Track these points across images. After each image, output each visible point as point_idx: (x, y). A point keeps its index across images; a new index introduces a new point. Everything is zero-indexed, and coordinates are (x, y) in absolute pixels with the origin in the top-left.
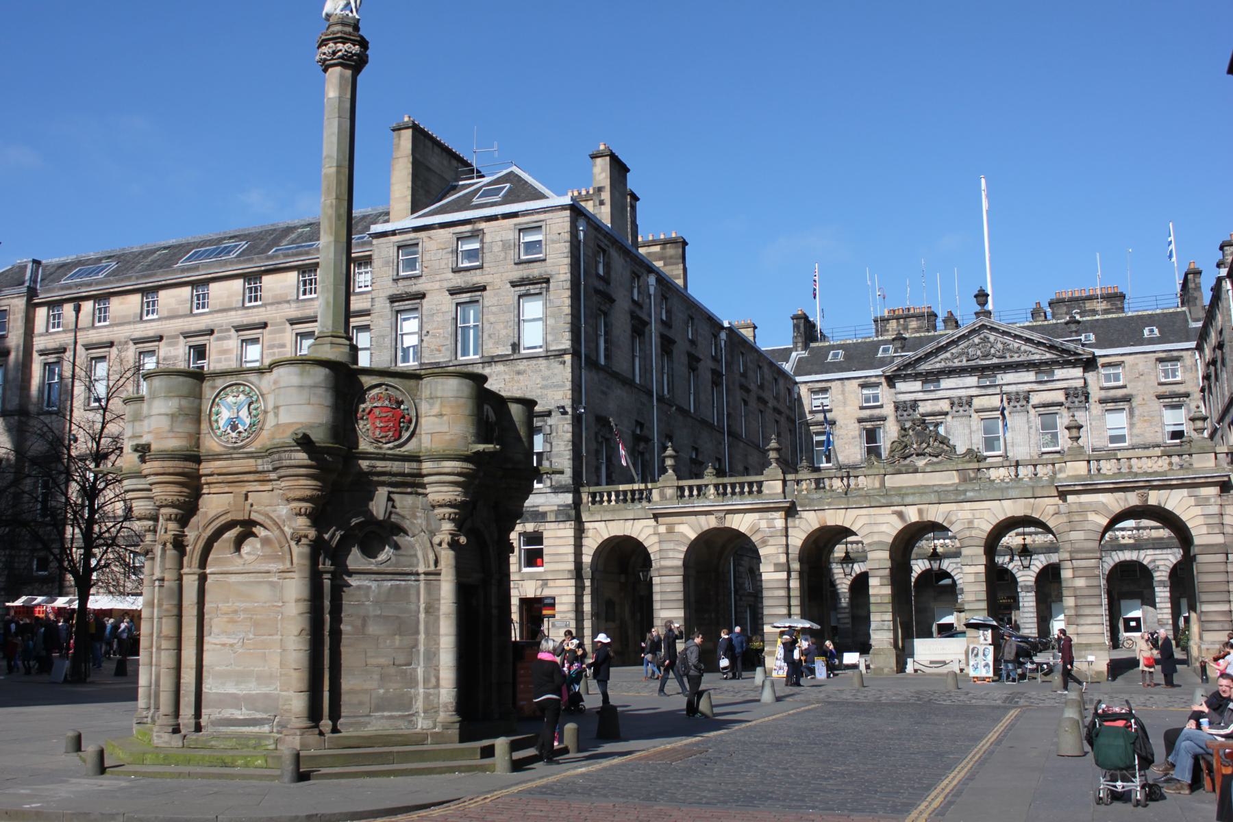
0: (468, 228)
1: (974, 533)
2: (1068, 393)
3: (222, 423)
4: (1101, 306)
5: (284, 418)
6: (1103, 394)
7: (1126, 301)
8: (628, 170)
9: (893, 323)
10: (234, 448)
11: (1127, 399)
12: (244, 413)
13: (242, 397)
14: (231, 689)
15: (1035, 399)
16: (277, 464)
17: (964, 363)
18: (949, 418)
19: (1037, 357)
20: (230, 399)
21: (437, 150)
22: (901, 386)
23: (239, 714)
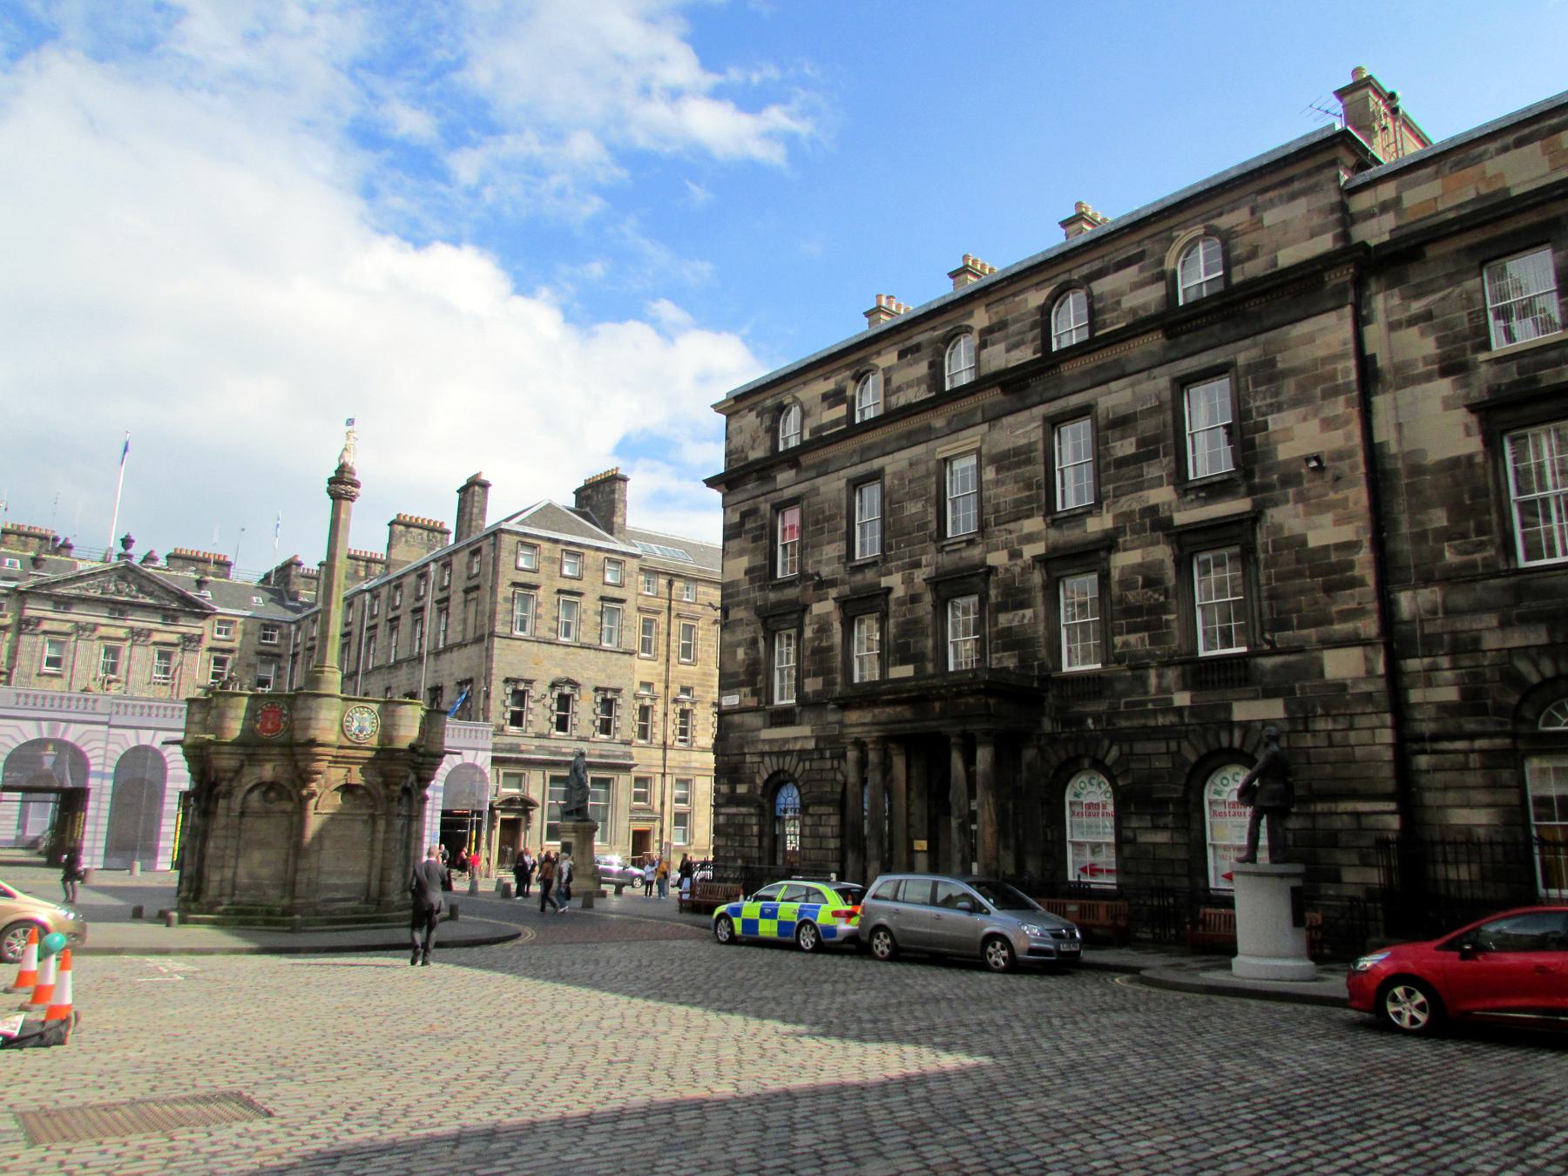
4: (212, 568)
12: (367, 724)
14: (335, 880)
15: (157, 637)
17: (98, 594)
23: (339, 896)
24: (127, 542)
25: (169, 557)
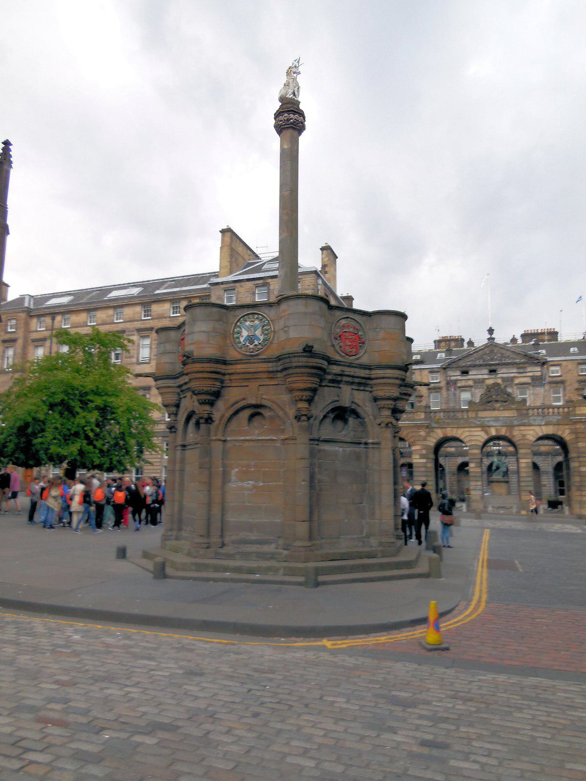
0: (261, 281)
1: (526, 442)
2: (533, 378)
3: (242, 339)
5: (293, 334)
6: (550, 379)
7: (559, 335)
8: (337, 258)
9: (443, 344)
10: (252, 356)
11: (562, 382)
12: (258, 333)
13: (257, 322)
15: (517, 381)
16: (287, 365)
17: (481, 363)
18: (473, 389)
19: (518, 361)
20: (248, 323)
21: (242, 244)
22: (450, 373)
23: (253, 537)
24: (491, 331)
25: (523, 336)
